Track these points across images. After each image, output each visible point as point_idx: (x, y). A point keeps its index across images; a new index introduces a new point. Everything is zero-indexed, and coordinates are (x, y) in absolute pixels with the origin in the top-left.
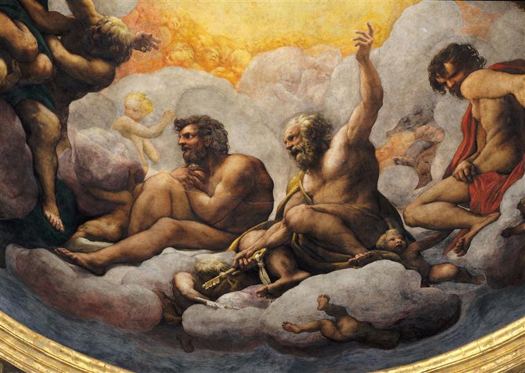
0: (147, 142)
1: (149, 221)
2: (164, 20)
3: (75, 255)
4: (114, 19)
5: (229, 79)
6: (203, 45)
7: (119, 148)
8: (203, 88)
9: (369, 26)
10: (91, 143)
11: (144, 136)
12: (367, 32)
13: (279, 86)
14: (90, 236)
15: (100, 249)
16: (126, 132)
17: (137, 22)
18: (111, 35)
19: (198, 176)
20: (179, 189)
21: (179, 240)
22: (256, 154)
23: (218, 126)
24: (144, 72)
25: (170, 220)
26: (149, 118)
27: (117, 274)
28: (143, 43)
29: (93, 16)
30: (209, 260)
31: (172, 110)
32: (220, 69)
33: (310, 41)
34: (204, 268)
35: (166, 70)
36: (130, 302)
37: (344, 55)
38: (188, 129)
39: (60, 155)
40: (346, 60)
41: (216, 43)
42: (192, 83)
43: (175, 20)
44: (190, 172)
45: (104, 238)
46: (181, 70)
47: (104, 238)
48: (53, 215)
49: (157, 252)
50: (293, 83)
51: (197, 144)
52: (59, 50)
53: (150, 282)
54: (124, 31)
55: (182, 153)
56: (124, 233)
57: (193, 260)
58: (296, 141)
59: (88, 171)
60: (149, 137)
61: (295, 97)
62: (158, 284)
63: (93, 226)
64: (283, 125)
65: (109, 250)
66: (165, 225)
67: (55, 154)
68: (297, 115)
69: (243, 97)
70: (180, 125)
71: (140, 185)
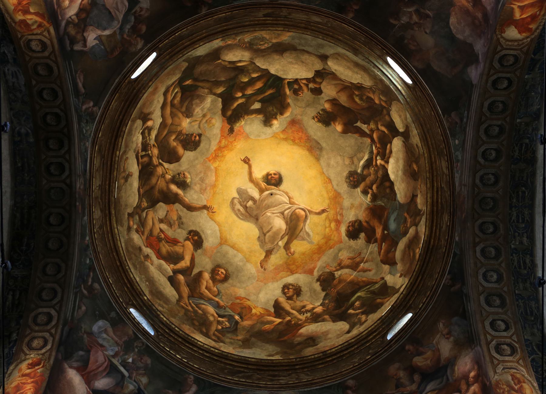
0: (198, 122)
1: (173, 115)
2: (237, 140)
3: (173, 86)
4: (243, 123)
5: (210, 157)
6: (224, 151)
7: (200, 112)
8: (209, 147)
9: (215, 212)
10: (206, 103)
11: (200, 122)
12: (213, 211)
13: (202, 175)
14: (177, 92)
15: (171, 95)
16: (204, 116)
17: (239, 131)
18: (238, 120)
19: (181, 137)
20: (179, 129)
21: (163, 125)
22: (182, 160)
23: (195, 149)
24: (222, 128)
25: (170, 123)
26: (206, 125)
27: (161, 100)
28: (231, 131)
29: (247, 116)
30: (154, 134)
31: (206, 134)
32: (214, 155)
33: (215, 190)
34: (152, 132)
35: (219, 136)
36: (151, 103)
37: (207, 201)
38: (197, 138)
39: (206, 91)
40: (205, 201)
41: (223, 156)
42: (212, 144)
43: (236, 144)
44: (183, 135)
45: (174, 98)
46: (218, 141)
47: (174, 98)
48: (188, 82)
49: (163, 116)
50: (202, 180)
51: (192, 139)
52: (240, 101)
53: (154, 110)
54: (238, 125)
55: (190, 133)
56: (172, 105)
57: (155, 128)
58: (183, 176)
59: (197, 99)
60: (200, 123)
61: (197, 179)
62: (153, 113)
63: (179, 95)
64: (189, 173)
65: (170, 98)
66: (169, 121)
67: (207, 89)
68: (191, 178)
69: (202, 160)
70: (200, 135)
71: (185, 115)
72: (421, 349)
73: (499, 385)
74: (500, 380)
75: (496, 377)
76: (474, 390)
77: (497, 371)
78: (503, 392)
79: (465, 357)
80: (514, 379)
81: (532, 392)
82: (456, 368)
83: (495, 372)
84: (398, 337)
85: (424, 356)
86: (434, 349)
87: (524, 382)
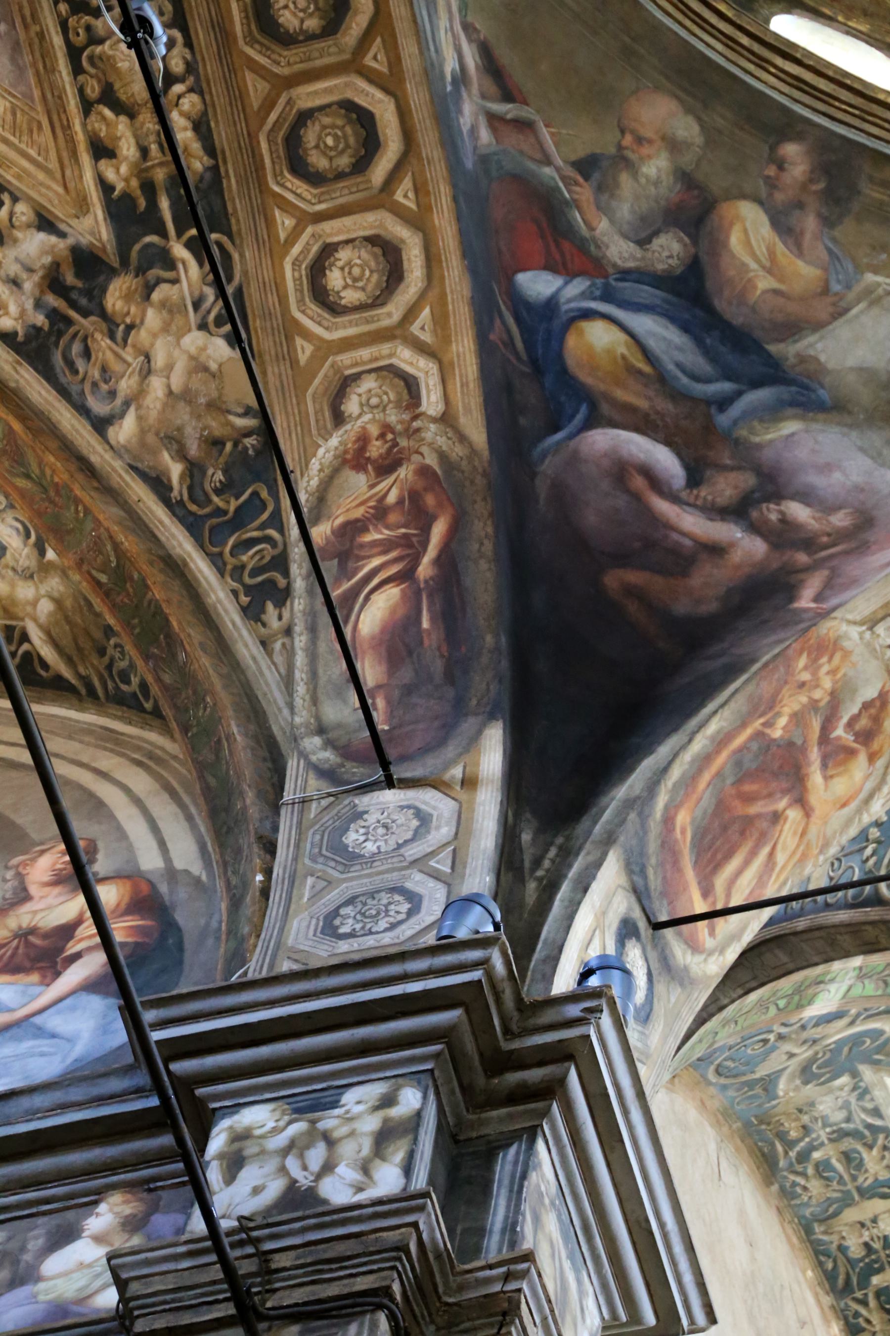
72: (810, 223)
73: (824, 659)
74: (847, 654)
75: (854, 632)
76: (732, 545)
77: (880, 629)
78: (802, 685)
79: (861, 449)
80: (873, 711)
81: (844, 805)
82: (790, 427)
83: (872, 623)
84: (822, 84)
85: (780, 247)
86: (836, 287)
87: (872, 758)
